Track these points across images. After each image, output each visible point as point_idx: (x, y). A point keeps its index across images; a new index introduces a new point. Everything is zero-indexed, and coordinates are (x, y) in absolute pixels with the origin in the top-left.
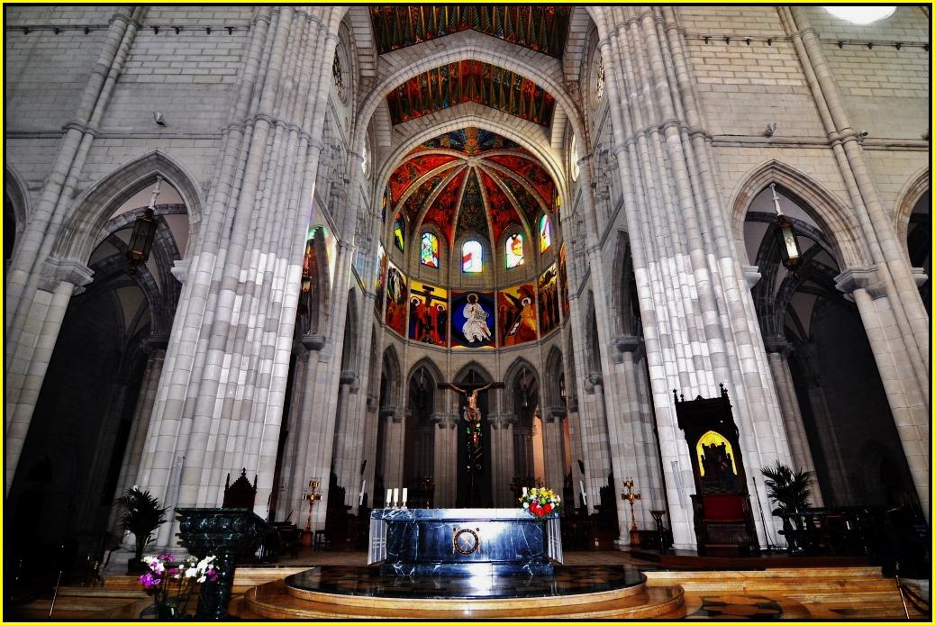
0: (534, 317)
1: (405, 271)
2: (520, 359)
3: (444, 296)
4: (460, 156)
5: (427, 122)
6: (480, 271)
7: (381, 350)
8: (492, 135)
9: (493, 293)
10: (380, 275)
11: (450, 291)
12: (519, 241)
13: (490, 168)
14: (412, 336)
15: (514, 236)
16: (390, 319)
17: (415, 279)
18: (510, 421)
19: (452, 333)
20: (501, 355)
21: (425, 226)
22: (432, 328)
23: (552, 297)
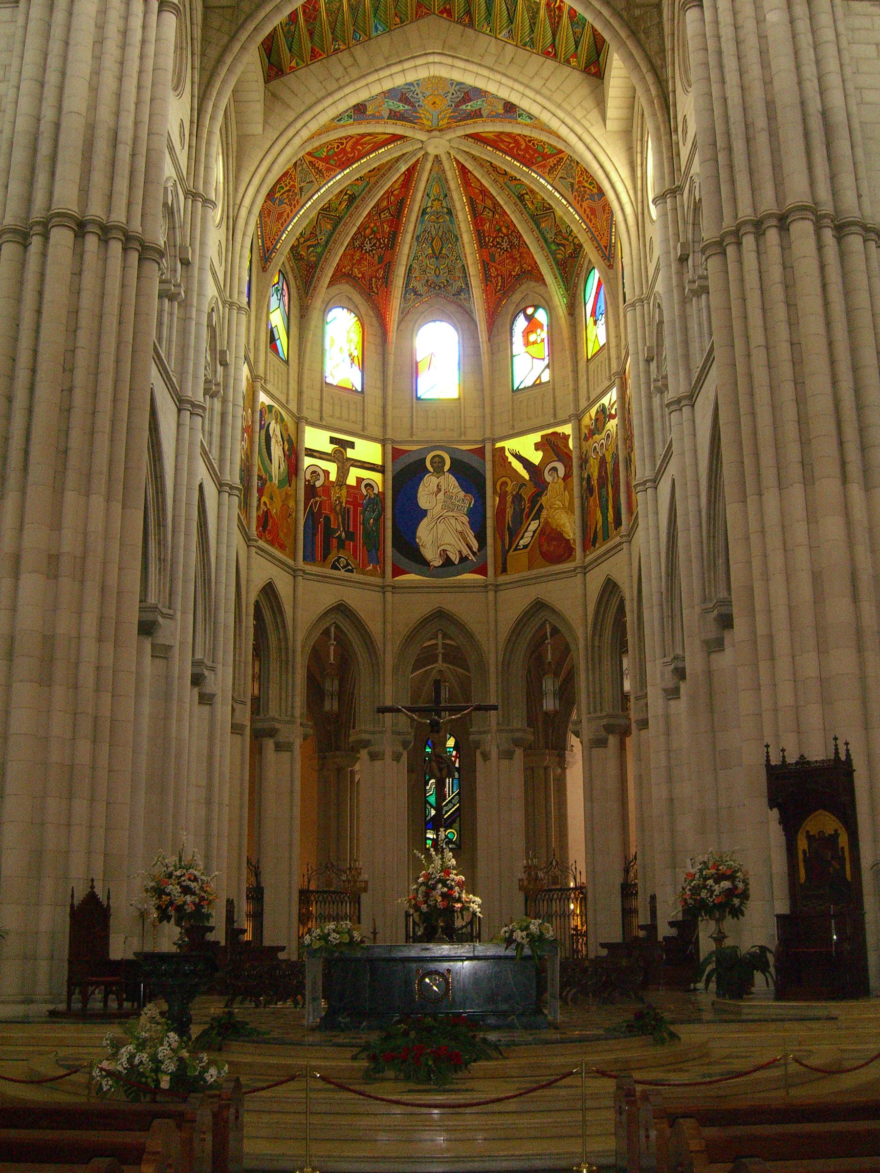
0: (570, 509)
1: (293, 407)
2: (539, 606)
3: (378, 461)
4: (408, 133)
5: (338, 72)
6: (456, 396)
7: (251, 596)
8: (480, 93)
9: (484, 447)
10: (244, 430)
11: (389, 447)
12: (541, 326)
13: (474, 158)
14: (309, 557)
15: (530, 311)
16: (265, 520)
17: (313, 425)
18: (517, 743)
19: (393, 546)
20: (502, 595)
21: (335, 289)
22: (351, 536)
23: (610, 467)
